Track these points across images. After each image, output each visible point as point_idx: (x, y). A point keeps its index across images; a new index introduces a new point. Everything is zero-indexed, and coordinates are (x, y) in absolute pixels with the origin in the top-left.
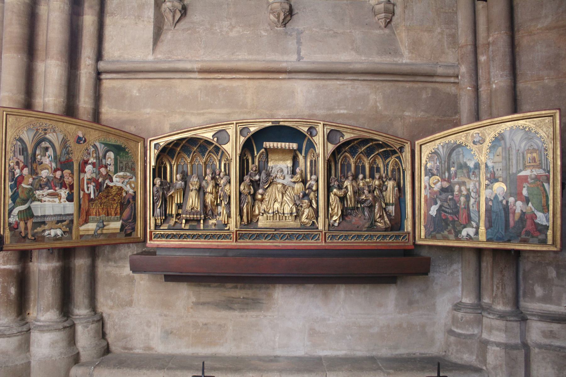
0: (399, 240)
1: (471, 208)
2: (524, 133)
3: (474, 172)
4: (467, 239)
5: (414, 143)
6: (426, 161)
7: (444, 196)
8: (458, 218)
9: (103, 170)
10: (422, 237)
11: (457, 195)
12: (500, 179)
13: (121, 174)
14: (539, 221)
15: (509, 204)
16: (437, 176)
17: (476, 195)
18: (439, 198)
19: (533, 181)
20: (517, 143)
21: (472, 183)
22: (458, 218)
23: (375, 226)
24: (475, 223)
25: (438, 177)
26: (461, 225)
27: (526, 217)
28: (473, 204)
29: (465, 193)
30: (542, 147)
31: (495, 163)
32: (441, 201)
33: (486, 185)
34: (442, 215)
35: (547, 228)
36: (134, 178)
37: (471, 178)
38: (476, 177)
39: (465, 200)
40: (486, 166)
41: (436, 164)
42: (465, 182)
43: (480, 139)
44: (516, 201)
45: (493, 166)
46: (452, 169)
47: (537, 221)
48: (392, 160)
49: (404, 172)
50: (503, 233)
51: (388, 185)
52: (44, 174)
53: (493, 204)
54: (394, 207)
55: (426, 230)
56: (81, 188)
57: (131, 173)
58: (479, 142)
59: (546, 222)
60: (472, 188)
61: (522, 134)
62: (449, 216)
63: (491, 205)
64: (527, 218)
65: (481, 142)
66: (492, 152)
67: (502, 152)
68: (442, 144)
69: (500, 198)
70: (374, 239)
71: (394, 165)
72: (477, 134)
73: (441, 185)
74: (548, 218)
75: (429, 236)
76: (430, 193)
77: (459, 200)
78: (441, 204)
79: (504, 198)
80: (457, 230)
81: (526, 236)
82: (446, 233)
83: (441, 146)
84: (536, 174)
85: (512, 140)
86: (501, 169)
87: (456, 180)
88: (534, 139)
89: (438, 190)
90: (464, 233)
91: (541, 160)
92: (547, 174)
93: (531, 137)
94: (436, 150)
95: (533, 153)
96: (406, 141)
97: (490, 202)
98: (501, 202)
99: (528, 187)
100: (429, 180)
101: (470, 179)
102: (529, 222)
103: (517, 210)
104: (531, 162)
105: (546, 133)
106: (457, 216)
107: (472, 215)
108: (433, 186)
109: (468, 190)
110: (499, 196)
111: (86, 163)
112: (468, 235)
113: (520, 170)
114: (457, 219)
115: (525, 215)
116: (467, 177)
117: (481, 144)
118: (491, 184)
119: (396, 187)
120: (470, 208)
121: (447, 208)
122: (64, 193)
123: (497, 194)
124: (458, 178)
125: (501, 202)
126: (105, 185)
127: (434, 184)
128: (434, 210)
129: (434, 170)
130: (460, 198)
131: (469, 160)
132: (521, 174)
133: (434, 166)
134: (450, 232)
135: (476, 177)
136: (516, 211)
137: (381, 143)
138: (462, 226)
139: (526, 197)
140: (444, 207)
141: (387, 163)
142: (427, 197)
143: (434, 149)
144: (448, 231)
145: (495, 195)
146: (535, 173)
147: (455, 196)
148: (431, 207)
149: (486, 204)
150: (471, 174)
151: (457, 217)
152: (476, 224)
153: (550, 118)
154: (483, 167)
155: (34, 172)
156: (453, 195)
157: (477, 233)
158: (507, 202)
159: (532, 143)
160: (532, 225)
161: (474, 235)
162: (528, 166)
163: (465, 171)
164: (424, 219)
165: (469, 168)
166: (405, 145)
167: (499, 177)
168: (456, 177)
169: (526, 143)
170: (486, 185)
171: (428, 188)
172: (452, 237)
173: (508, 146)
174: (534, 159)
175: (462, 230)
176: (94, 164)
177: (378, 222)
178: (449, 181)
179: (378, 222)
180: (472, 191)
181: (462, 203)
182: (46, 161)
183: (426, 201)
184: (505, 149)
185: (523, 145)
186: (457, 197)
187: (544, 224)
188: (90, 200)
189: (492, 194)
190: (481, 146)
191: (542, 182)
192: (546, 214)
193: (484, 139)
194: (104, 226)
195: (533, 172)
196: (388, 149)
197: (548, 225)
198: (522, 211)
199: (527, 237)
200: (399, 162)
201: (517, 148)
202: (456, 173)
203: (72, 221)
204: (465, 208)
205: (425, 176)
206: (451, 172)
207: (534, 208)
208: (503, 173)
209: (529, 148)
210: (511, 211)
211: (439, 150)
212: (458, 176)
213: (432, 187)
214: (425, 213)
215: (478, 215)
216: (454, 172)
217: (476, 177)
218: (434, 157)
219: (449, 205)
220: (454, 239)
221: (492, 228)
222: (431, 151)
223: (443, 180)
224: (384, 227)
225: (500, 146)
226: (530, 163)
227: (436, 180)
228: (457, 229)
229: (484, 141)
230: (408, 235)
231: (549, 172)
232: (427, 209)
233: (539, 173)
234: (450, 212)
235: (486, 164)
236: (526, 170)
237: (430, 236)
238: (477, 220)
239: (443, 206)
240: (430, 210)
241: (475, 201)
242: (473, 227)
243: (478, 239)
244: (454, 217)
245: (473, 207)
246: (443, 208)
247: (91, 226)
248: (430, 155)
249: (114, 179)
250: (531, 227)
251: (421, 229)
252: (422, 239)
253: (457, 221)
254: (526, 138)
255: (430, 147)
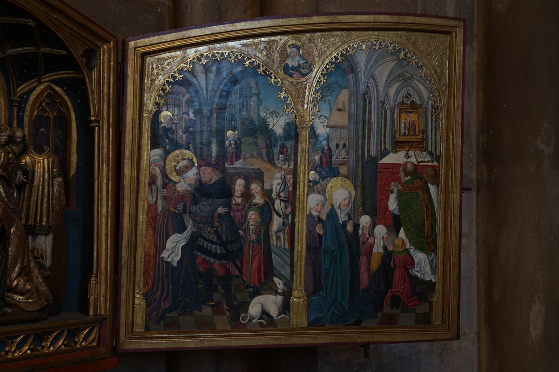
0: (76, 343)
1: (274, 242)
2: (395, 62)
3: (283, 147)
4: (261, 324)
5: (125, 45)
6: (157, 104)
7: (205, 206)
8: (240, 271)
10: (136, 329)
11: (239, 205)
12: (343, 170)
14: (418, 271)
15: (360, 232)
16: (188, 149)
17: (286, 207)
18: (190, 213)
19: (409, 178)
20: (381, 87)
21: (278, 175)
22: (240, 271)
23: (8, 305)
24: (281, 282)
25: (189, 154)
26: (248, 287)
27: (394, 262)
28: (278, 231)
29: (258, 200)
30: (428, 101)
31: (332, 127)
32: (194, 221)
33: (309, 181)
34: (198, 261)
35: (431, 285)
37: (277, 162)
38: (287, 160)
39: (259, 220)
40: (313, 134)
41: (185, 116)
42: (263, 172)
43: (302, 62)
44: (374, 225)
45: (328, 136)
46: (229, 133)
47: (415, 272)
48: (42, 87)
49: (94, 127)
50: (346, 304)
51: (33, 166)
53: (325, 232)
54: (50, 237)
55: (148, 306)
58: (297, 69)
59: (430, 273)
60: (279, 187)
61: (392, 65)
62: (216, 263)
63: (321, 233)
64: (395, 267)
65: (305, 71)
66: (327, 99)
67: (350, 103)
68: (204, 61)
69: (342, 217)
70: (7, 353)
71: (44, 104)
72: (295, 50)
73: (198, 174)
74: (434, 266)
75: (158, 323)
76: (165, 198)
77: (245, 217)
78: (195, 230)
79: (350, 218)
80: (236, 303)
81: (392, 309)
82: (207, 311)
83: (202, 68)
84: (416, 163)
85: (372, 76)
86: (344, 146)
87: (238, 164)
88: (415, 81)
89: (189, 189)
90: (254, 309)
91: (425, 131)
92: (435, 163)
93: (409, 75)
94: (188, 76)
95: (411, 112)
96: (106, 35)
97: (318, 225)
98: (344, 225)
99: (399, 191)
100: (165, 160)
101: (274, 165)
102: (398, 274)
103: (375, 245)
104: (407, 133)
105: (436, 71)
106: (238, 263)
107: (275, 259)
108: (174, 177)
109: (267, 193)
110: (338, 211)
112: (265, 313)
113: (385, 149)
114: (237, 273)
115: (390, 259)
116: (266, 158)
117: (304, 75)
118: (322, 182)
119: (59, 176)
120: (271, 242)
121: (211, 242)
123: (336, 207)
124: (245, 159)
125: (344, 225)
127: (176, 171)
128: (174, 247)
129: (180, 132)
130: (246, 214)
131: (272, 113)
132: (385, 161)
133: (180, 119)
134: (217, 310)
135: (289, 161)
136: (375, 250)
137: (31, 23)
138: (251, 290)
139: (394, 216)
140: (205, 238)
141: (19, 97)
142: (156, 209)
143: (180, 71)
144: (212, 306)
145: (330, 207)
146: (413, 160)
147: (234, 207)
148: (167, 238)
149: (310, 231)
150: (276, 150)
151: (236, 266)
152: (285, 284)
153: (444, 36)
154: (305, 134)
156: (229, 205)
157: (286, 308)
158: (357, 226)
159: (410, 88)
160: (405, 281)
161: (279, 315)
162: (400, 142)
163: (262, 143)
164: (146, 273)
165: (271, 137)
166: (99, 48)
167: (341, 164)
168: (238, 158)
169: (398, 88)
170: (309, 181)
171: (159, 182)
172: (222, 321)
173: (362, 89)
174: (412, 127)
175: (250, 302)
177: (15, 290)
178: (219, 166)
179: (15, 290)
180: (278, 195)
181: (252, 228)
183: (153, 219)
184: (353, 95)
185: (392, 91)
186: (238, 210)
187: (427, 279)
189: (323, 206)
190: (303, 79)
191: (426, 182)
192: (431, 254)
193: (311, 64)
195: (409, 157)
196: (42, 49)
197: (434, 281)
198: (385, 247)
199: (394, 311)
200: (66, 98)
201: (382, 97)
202: (238, 146)
204: (258, 241)
205: (154, 145)
206: (227, 142)
207: (409, 240)
208: (348, 154)
209: (405, 99)
210: (363, 249)
211: (195, 77)
212: (243, 153)
213: (171, 181)
214: (147, 255)
215: (288, 260)
216: (233, 142)
217: (289, 161)
218: (179, 93)
219: (216, 232)
220: (228, 327)
221: (321, 293)
222: (173, 77)
223: (204, 161)
224: (36, 308)
225: (346, 88)
226: (404, 135)
227: (184, 163)
228: (236, 299)
229: (310, 67)
230: (98, 327)
231: (438, 159)
232: (156, 246)
233: (420, 160)
234: (218, 251)
235: (312, 127)
236: (396, 152)
237: (162, 323)
238: (286, 272)
239: (202, 236)
240: (164, 247)
241: (284, 224)
242: (276, 293)
243: (289, 320)
244: (230, 266)
245: (278, 238)
246: (201, 241)
248: (167, 87)
250: (402, 287)
251: (134, 304)
252: (138, 333)
253: (237, 276)
254: (399, 76)
255: (168, 64)
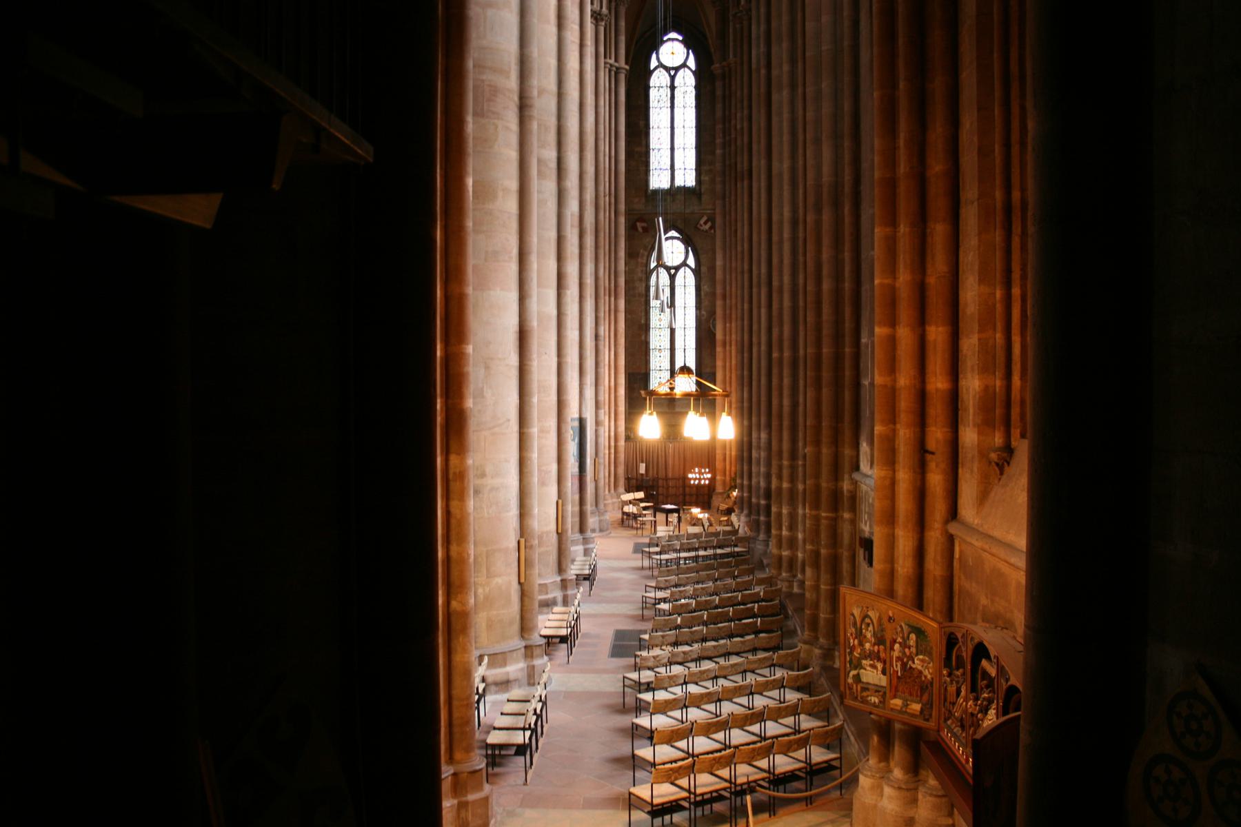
9: (907, 650)
13: (921, 657)
36: (932, 663)
52: (867, 646)
56: (891, 665)
57: (929, 658)
111: (894, 641)
122: (880, 666)
126: (908, 666)
155: (861, 644)
176: (900, 643)
182: (869, 635)
188: (898, 678)
194: (908, 705)
203: (885, 693)
247: (897, 702)
249: (916, 661)
